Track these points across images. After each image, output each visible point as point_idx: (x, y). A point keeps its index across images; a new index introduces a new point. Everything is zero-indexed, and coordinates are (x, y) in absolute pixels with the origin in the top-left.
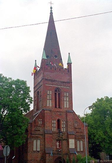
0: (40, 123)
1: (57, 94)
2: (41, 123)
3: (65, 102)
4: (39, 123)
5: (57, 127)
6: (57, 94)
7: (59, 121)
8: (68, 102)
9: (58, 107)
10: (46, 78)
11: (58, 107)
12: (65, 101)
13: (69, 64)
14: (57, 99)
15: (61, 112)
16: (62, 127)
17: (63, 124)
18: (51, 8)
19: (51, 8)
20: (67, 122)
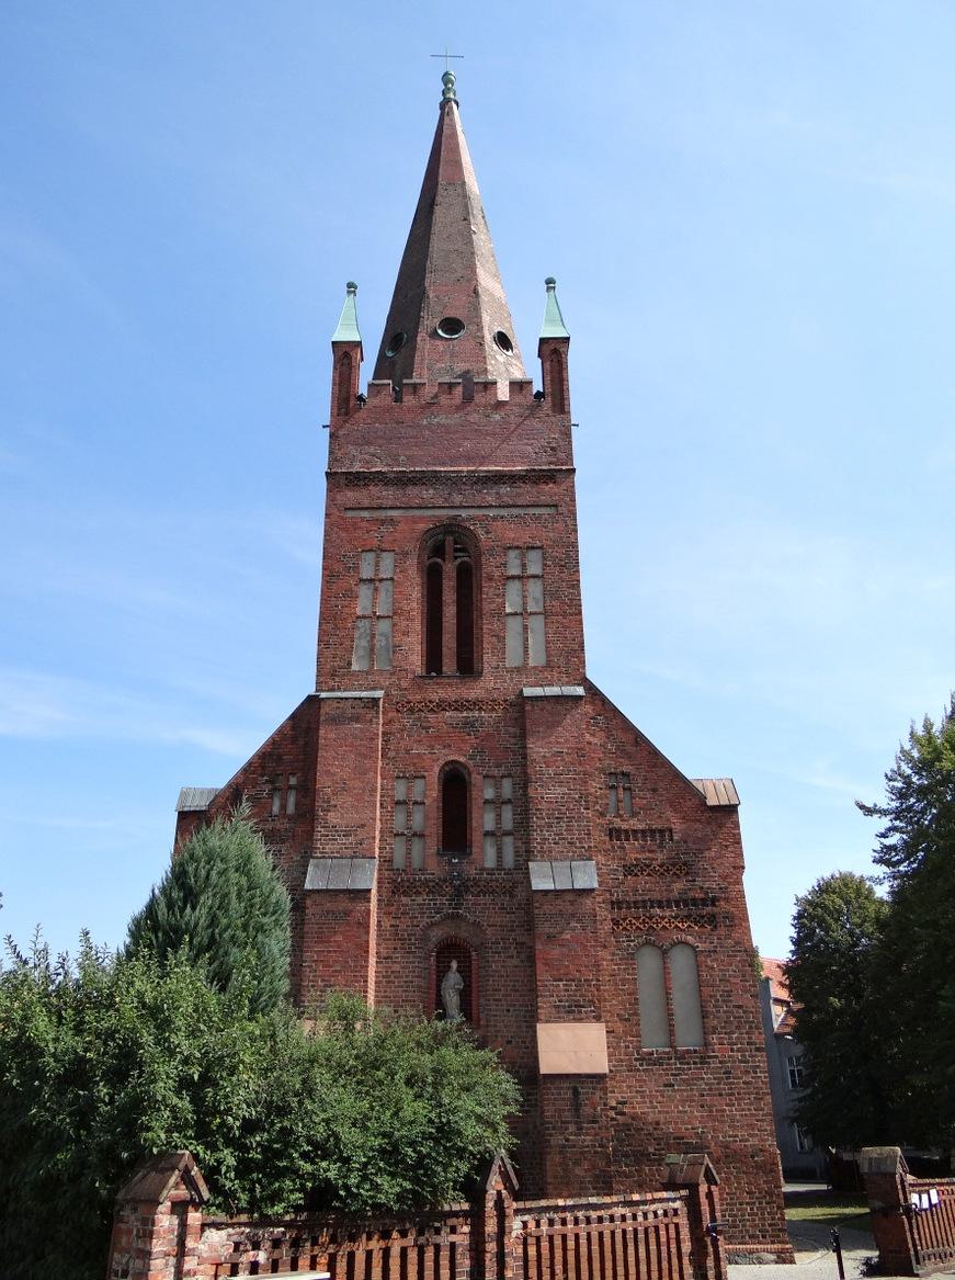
0: (283, 807)
1: (449, 569)
2: (291, 809)
3: (514, 625)
4: (276, 809)
5: (434, 829)
6: (449, 569)
7: (455, 784)
8: (537, 624)
9: (449, 665)
10: (357, 468)
11: (449, 665)
12: (510, 619)
13: (553, 352)
14: (450, 612)
15: (476, 704)
16: (489, 824)
17: (497, 803)
18: (446, 79)
19: (446, 79)
20: (524, 783)
